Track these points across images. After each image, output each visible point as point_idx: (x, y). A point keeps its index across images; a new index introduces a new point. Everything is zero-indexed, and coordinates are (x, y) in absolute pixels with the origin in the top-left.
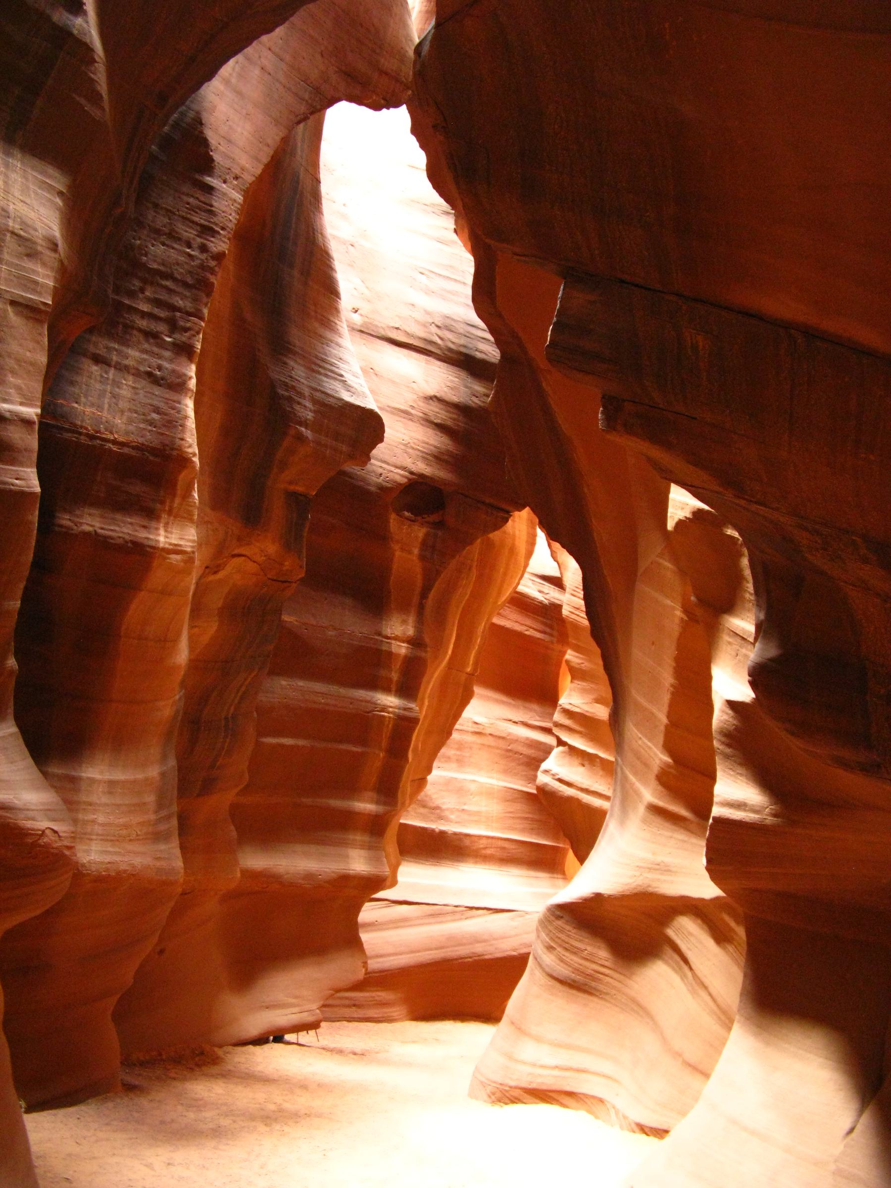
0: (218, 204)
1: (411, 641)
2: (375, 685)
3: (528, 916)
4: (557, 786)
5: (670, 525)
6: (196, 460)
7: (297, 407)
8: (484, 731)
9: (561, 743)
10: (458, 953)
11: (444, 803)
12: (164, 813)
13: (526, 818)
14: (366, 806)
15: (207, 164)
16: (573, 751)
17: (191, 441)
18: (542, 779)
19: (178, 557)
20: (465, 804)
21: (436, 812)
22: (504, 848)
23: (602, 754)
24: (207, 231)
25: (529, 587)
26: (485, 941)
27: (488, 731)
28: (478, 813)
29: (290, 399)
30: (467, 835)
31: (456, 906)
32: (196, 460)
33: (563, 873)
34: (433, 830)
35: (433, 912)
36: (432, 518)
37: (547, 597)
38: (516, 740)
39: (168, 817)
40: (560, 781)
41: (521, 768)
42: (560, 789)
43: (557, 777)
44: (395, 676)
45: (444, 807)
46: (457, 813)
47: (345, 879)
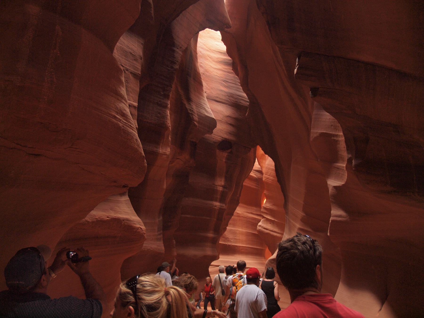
0: (176, 55)
1: (224, 187)
2: (212, 199)
4: (263, 229)
5: (311, 139)
6: (170, 128)
7: (194, 116)
9: (263, 217)
12: (159, 233)
14: (211, 235)
15: (173, 45)
16: (267, 220)
17: (169, 122)
18: (258, 228)
19: (165, 156)
21: (227, 239)
23: (276, 220)
24: (173, 63)
25: (252, 174)
28: (239, 239)
29: (192, 114)
30: (236, 246)
32: (170, 128)
33: (264, 257)
34: (226, 245)
36: (229, 151)
38: (250, 218)
39: (160, 234)
40: (264, 228)
44: (219, 197)
47: (205, 257)
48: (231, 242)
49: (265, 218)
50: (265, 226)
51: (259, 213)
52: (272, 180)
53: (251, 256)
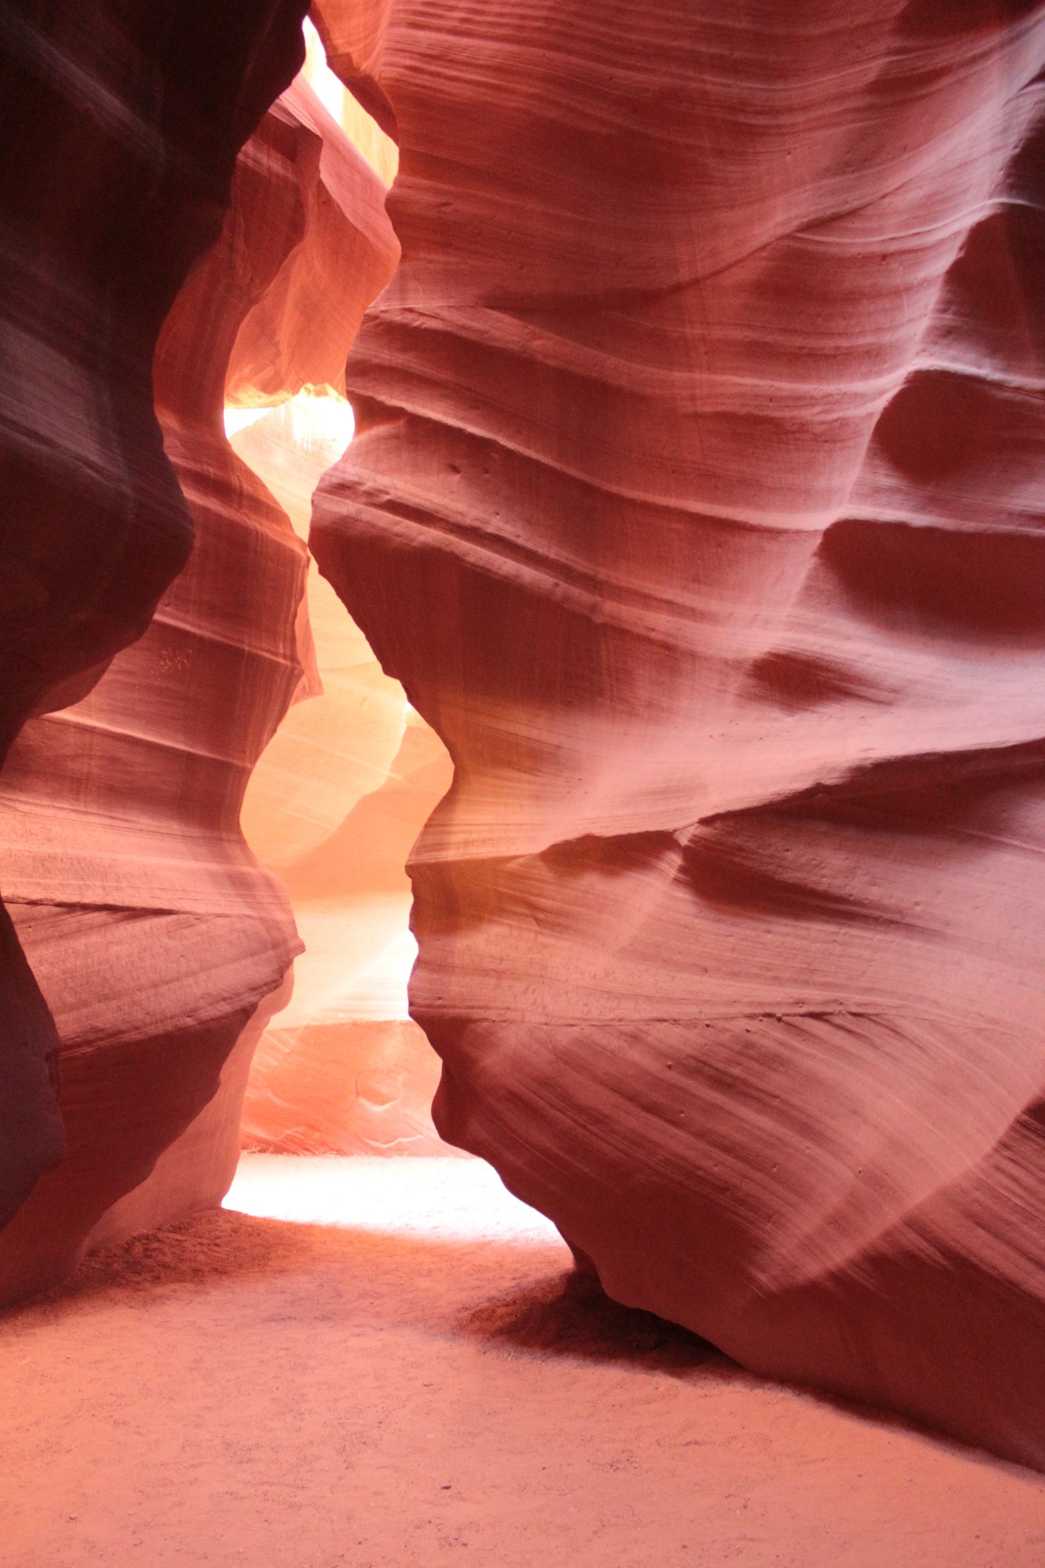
3: (203, 927)
22: (114, 760)
23: (503, 441)
40: (396, 507)
42: (397, 529)
43: (388, 497)
49: (395, 414)
52: (499, 70)
53: (145, 821)
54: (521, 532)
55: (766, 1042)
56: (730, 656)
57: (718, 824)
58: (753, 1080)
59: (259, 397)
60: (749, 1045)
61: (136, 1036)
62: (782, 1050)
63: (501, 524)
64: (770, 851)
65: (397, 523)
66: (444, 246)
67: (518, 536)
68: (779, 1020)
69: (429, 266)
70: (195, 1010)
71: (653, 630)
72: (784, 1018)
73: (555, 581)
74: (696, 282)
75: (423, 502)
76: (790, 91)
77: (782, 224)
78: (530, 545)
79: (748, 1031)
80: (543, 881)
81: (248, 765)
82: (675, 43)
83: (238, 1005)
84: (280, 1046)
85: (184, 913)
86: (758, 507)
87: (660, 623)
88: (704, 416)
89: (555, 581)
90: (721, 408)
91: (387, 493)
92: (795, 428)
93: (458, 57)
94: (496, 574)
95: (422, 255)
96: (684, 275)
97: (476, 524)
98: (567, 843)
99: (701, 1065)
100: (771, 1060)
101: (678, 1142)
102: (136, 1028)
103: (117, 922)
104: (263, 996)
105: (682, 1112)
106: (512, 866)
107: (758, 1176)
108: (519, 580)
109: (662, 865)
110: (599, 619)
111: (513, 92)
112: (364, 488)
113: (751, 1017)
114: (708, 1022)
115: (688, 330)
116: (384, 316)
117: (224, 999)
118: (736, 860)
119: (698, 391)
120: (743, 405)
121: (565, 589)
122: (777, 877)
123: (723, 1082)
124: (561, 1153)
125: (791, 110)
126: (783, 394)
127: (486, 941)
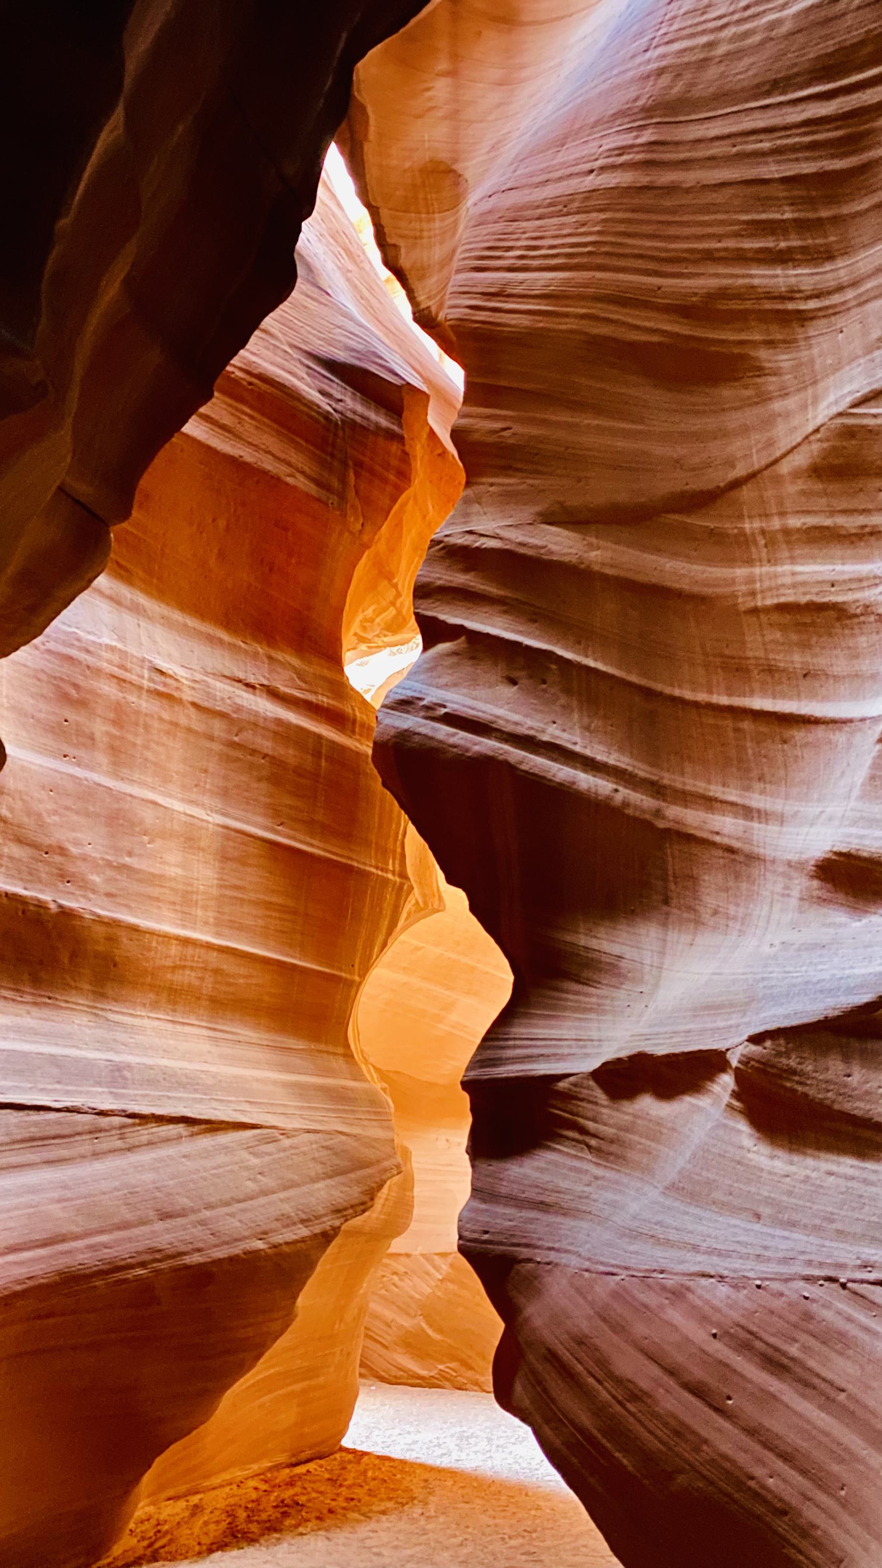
3: (286, 1142)
4: (443, 732)
8: (175, 694)
10: (107, 1254)
11: (77, 843)
13: (268, 905)
16: (482, 647)
20: (130, 854)
22: (217, 971)
23: (560, 652)
26: (182, 1213)
27: (187, 695)
31: (102, 1113)
34: (41, 906)
35: (34, 1131)
37: (339, 407)
38: (255, 723)
40: (453, 720)
41: (264, 785)
42: (452, 740)
43: (443, 711)
45: (74, 850)
46: (109, 873)
48: (86, 886)
49: (456, 632)
50: (458, 700)
51: (324, 700)
53: (247, 1033)
54: (578, 740)
55: (828, 1315)
56: (794, 857)
57: (768, 1044)
58: (812, 1363)
59: (385, 636)
60: (808, 1316)
61: (196, 1259)
62: (849, 1327)
63: (558, 733)
64: (829, 1075)
65: (454, 735)
66: (506, 469)
67: (575, 744)
68: (844, 1286)
69: (491, 489)
70: (265, 1233)
71: (718, 833)
72: (849, 1285)
73: (615, 786)
74: (752, 476)
75: (480, 714)
76: (838, 270)
77: (836, 402)
78: (588, 752)
79: (806, 1298)
80: (596, 1103)
81: (357, 978)
82: (719, 245)
83: (317, 1229)
84: (433, 1271)
85: (266, 1127)
86: (825, 699)
87: (726, 826)
88: (767, 610)
89: (615, 786)
90: (782, 600)
91: (445, 707)
92: (858, 611)
93: (515, 291)
94: (550, 780)
95: (484, 480)
96: (740, 471)
97: (532, 733)
98: (619, 1060)
99: (751, 1337)
100: (835, 1340)
101: (724, 1439)
102: (199, 1250)
103: (192, 1135)
104: (346, 1220)
105: (729, 1398)
106: (562, 1085)
107: (822, 1497)
108: (575, 787)
109: (716, 1088)
110: (661, 824)
111: (566, 315)
112: (422, 703)
113: (807, 1279)
114: (758, 1282)
115: (747, 526)
116: (447, 539)
117: (302, 1221)
118: (788, 1084)
119: (758, 585)
120: (805, 594)
121: (624, 794)
122: (836, 1107)
123: (776, 1363)
124: (595, 1432)
125: (840, 289)
126: (846, 577)
127: (544, 1169)
